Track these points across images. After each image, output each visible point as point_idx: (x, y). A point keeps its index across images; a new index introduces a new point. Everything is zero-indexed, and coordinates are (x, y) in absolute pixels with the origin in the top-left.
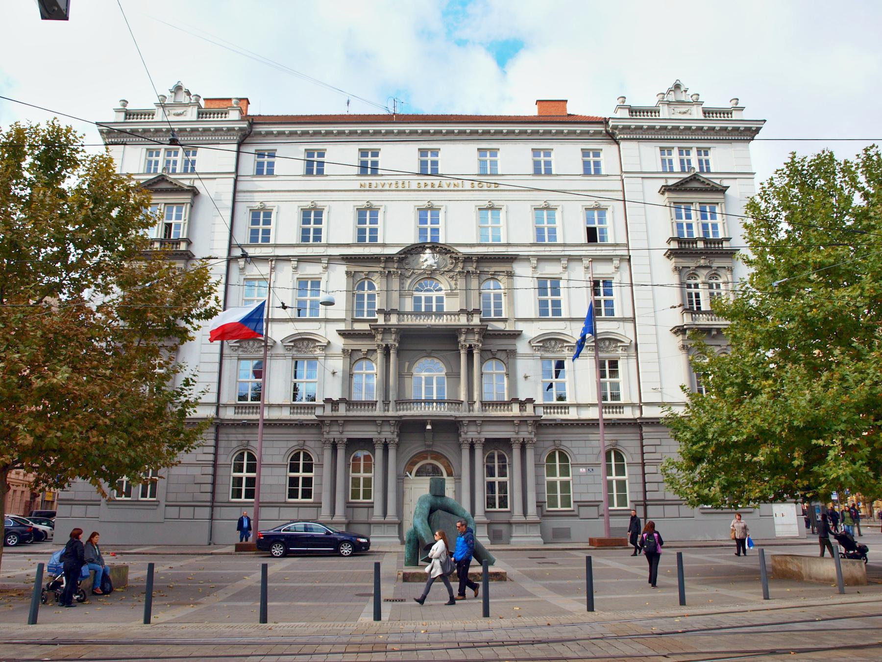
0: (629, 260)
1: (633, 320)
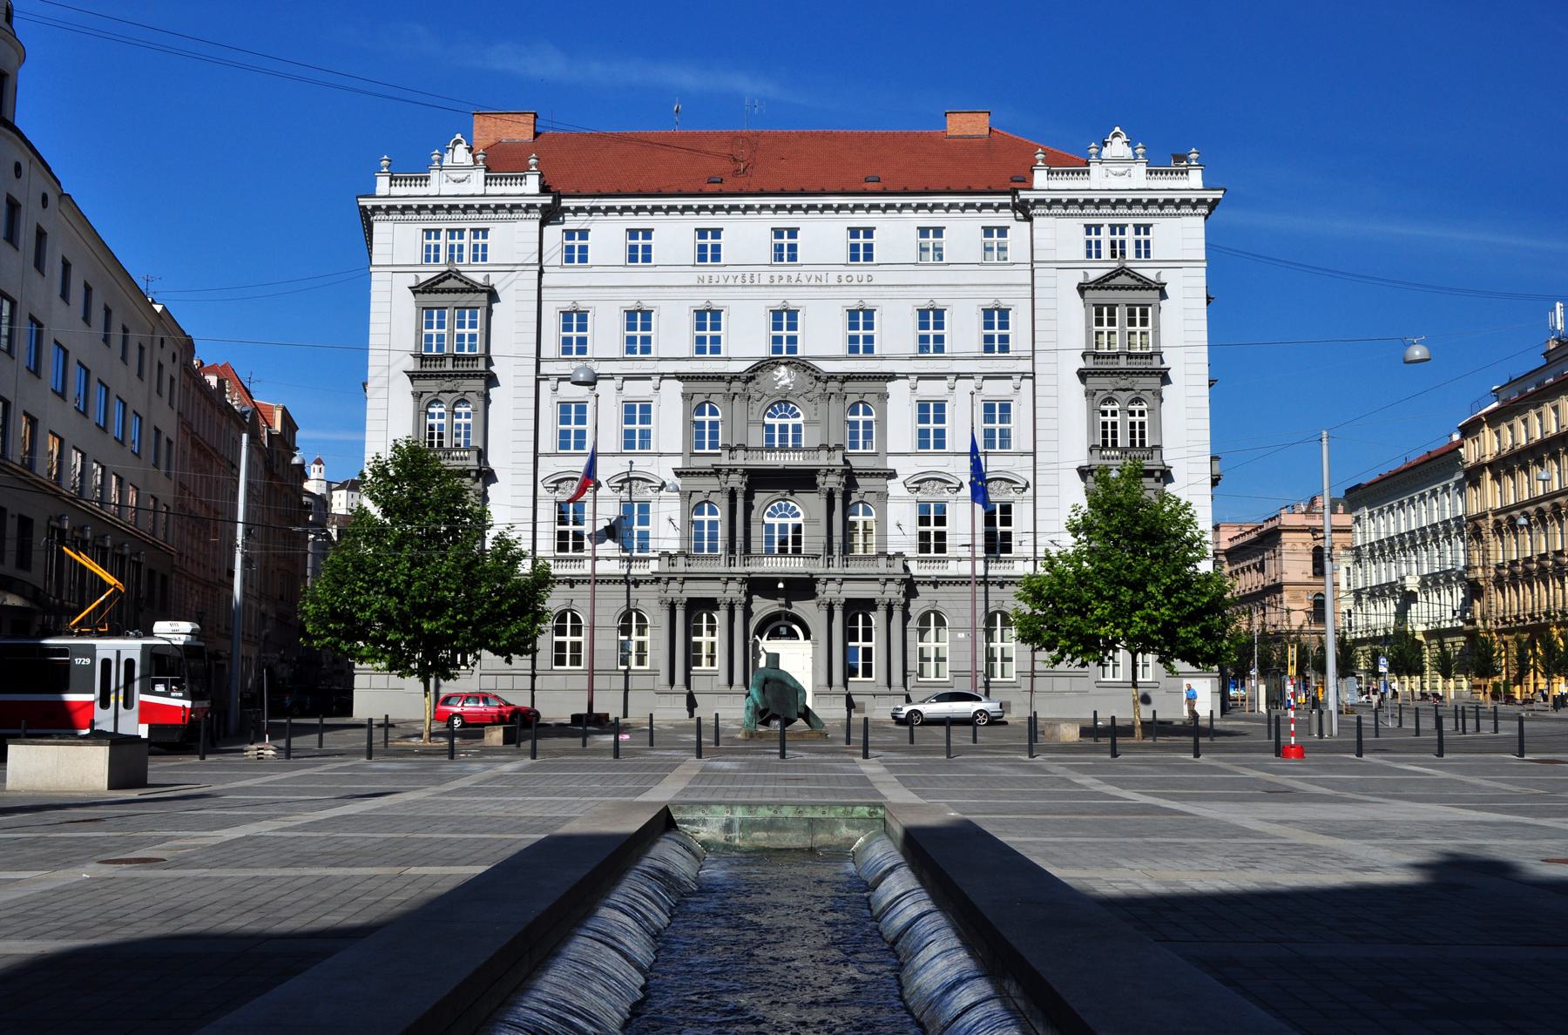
0: (1033, 378)
1: (1034, 454)
